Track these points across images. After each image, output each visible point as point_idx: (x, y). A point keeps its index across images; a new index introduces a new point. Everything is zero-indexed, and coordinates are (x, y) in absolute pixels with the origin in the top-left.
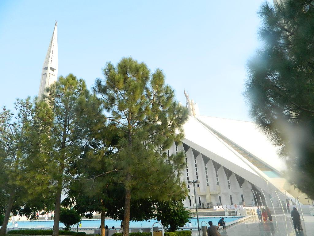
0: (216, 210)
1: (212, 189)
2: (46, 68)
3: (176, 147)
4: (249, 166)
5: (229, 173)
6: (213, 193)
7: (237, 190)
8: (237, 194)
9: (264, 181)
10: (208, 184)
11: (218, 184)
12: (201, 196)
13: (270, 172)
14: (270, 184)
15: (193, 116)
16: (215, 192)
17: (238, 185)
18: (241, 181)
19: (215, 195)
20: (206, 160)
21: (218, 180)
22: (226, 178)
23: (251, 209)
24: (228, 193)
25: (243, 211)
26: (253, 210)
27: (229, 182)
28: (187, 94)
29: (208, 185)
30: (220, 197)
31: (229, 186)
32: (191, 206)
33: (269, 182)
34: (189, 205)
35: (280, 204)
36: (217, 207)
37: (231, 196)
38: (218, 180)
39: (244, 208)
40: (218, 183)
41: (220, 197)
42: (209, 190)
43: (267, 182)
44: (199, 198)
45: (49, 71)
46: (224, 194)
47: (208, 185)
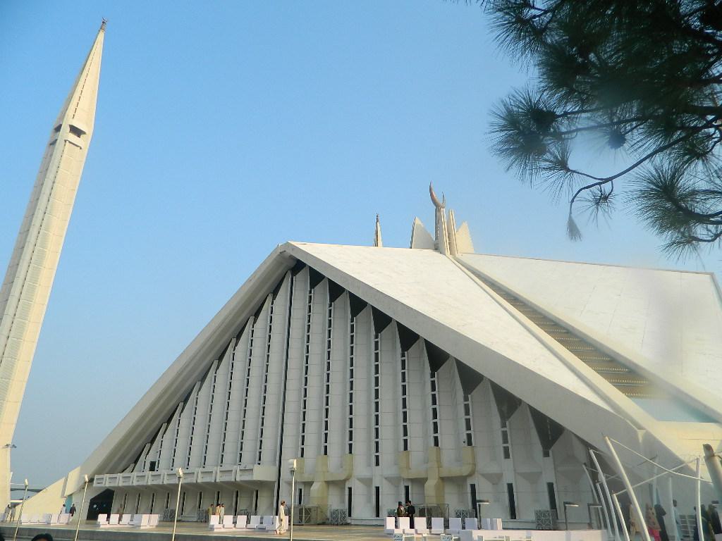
1: (451, 458)
2: (58, 129)
3: (352, 321)
5: (508, 403)
6: (453, 474)
8: (532, 478)
10: (436, 439)
11: (470, 443)
15: (448, 253)
18: (549, 432)
19: (458, 481)
20: (437, 358)
21: (468, 428)
22: (497, 420)
27: (505, 435)
28: (440, 201)
29: (436, 444)
30: (473, 487)
32: (378, 515)
33: (647, 432)
34: (375, 514)
36: (404, 521)
37: (510, 487)
40: (469, 436)
42: (439, 461)
43: (640, 434)
44: (407, 488)
45: (65, 133)
46: (486, 476)
47: (436, 444)
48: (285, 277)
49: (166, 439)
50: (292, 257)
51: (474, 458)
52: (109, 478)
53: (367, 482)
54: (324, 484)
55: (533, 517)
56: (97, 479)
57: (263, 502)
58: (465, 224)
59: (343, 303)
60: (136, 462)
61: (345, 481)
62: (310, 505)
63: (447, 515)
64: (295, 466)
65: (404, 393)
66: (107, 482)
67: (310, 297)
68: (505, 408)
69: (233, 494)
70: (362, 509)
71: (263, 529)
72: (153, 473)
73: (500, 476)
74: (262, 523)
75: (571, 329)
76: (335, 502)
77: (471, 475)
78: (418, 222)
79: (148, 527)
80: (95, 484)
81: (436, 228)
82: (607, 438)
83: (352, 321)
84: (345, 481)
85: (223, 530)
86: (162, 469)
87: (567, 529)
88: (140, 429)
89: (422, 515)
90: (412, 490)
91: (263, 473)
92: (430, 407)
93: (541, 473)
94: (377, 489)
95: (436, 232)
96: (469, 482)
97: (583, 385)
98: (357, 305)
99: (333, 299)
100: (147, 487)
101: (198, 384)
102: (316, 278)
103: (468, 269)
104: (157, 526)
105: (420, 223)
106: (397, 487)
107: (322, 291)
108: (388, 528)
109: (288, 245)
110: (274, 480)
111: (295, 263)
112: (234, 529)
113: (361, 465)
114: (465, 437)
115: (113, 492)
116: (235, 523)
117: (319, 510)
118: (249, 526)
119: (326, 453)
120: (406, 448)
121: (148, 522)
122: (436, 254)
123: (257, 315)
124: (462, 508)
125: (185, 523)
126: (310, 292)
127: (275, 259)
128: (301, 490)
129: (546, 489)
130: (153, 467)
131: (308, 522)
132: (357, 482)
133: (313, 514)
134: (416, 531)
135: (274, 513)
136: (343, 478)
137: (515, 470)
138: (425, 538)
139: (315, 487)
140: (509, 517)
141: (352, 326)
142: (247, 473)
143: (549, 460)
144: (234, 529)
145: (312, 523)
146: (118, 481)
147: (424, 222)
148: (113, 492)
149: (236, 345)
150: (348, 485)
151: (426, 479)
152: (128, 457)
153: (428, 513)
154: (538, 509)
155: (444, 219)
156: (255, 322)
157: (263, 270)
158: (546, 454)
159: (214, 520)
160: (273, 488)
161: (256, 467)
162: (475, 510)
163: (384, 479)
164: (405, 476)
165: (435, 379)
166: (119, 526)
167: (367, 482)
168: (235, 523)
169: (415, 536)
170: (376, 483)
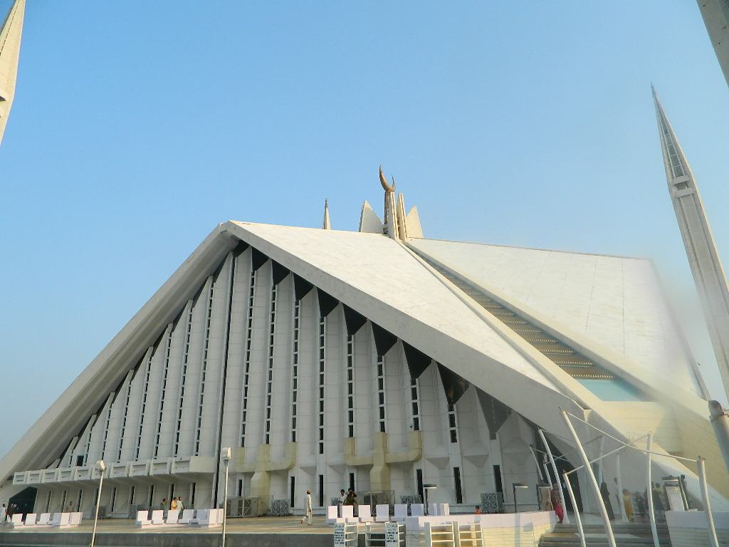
0: (332, 524)
1: (398, 443)
4: (481, 317)
5: (453, 385)
7: (483, 450)
8: (478, 461)
9: (577, 407)
10: (382, 424)
12: (358, 468)
13: (606, 385)
14: (595, 418)
15: (397, 238)
16: (402, 456)
17: (485, 431)
18: (497, 413)
19: (404, 467)
21: (415, 412)
23: (468, 528)
24: (449, 459)
25: (420, 536)
26: (474, 533)
28: (389, 185)
29: (383, 429)
30: (419, 472)
31: (453, 434)
32: (321, 504)
35: (566, 491)
36: (348, 510)
37: (456, 470)
38: (415, 412)
39: (422, 520)
40: (416, 421)
41: (419, 472)
42: (385, 447)
43: (586, 413)
44: (352, 476)
47: (383, 429)
48: (226, 256)
49: (96, 432)
50: (233, 237)
51: (421, 442)
52: (32, 475)
53: (311, 470)
54: (266, 476)
55: (479, 501)
56: (17, 476)
57: (201, 496)
58: (414, 210)
59: (287, 286)
60: (62, 457)
61: (287, 471)
62: (250, 497)
63: (392, 503)
64: (229, 455)
65: (350, 378)
66: (27, 479)
67: (253, 279)
68: (451, 395)
69: (148, 489)
70: (306, 499)
71: (195, 524)
72: (80, 468)
73: (447, 460)
74: (195, 517)
75: (518, 313)
76: (277, 493)
77: (418, 459)
78: (367, 205)
79: (69, 526)
80: (14, 482)
81: (386, 212)
82: (564, 412)
83: (297, 304)
84: (287, 471)
85: (152, 526)
86: (90, 464)
87: (516, 512)
88: (65, 422)
89: (366, 502)
90: (357, 478)
91: (200, 464)
92: (377, 392)
93: (488, 456)
94: (321, 477)
95: (385, 216)
96: (416, 467)
97: (530, 367)
98: (303, 287)
99: (277, 280)
100: (74, 483)
101: (131, 372)
102: (259, 259)
103: (417, 253)
104: (80, 525)
105: (369, 206)
106: (342, 474)
107: (265, 272)
108: (329, 518)
109: (229, 224)
110: (212, 471)
111: (237, 244)
112: (164, 525)
113: (304, 454)
114: (412, 422)
115: (36, 490)
116: (165, 518)
117: (260, 502)
118: (180, 521)
119: (268, 442)
120: (351, 434)
121: (69, 522)
122: (386, 238)
123: (195, 298)
124: (407, 494)
125: (113, 521)
126: (253, 274)
127: (215, 239)
128: (241, 481)
129: (492, 471)
130: (80, 461)
131: (248, 514)
132: (299, 470)
133: (253, 506)
134: (360, 520)
135: (213, 505)
136: (285, 467)
137: (461, 454)
138: (368, 527)
139: (255, 478)
140: (455, 502)
141: (297, 309)
142: (183, 465)
143: (496, 442)
144: (164, 525)
145: (252, 514)
146: (41, 477)
147: (374, 206)
148: (36, 490)
149: (173, 330)
150: (290, 475)
151: (372, 465)
152: (52, 453)
153: (372, 501)
154: (485, 492)
155: (394, 203)
156: (193, 306)
157: (203, 249)
158: (493, 437)
159: (142, 516)
160: (211, 480)
161: (193, 459)
162: (421, 496)
163: (328, 467)
164: (350, 463)
165: (382, 363)
166: (36, 526)
167: (311, 470)
168: (165, 518)
169: (358, 525)
170: (320, 472)
